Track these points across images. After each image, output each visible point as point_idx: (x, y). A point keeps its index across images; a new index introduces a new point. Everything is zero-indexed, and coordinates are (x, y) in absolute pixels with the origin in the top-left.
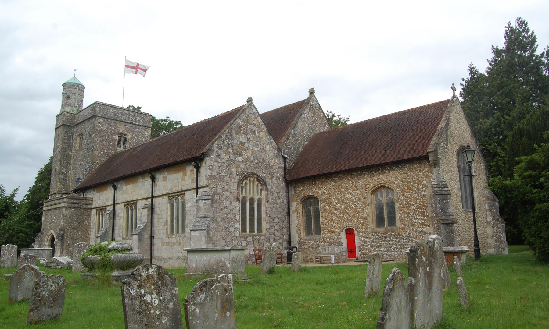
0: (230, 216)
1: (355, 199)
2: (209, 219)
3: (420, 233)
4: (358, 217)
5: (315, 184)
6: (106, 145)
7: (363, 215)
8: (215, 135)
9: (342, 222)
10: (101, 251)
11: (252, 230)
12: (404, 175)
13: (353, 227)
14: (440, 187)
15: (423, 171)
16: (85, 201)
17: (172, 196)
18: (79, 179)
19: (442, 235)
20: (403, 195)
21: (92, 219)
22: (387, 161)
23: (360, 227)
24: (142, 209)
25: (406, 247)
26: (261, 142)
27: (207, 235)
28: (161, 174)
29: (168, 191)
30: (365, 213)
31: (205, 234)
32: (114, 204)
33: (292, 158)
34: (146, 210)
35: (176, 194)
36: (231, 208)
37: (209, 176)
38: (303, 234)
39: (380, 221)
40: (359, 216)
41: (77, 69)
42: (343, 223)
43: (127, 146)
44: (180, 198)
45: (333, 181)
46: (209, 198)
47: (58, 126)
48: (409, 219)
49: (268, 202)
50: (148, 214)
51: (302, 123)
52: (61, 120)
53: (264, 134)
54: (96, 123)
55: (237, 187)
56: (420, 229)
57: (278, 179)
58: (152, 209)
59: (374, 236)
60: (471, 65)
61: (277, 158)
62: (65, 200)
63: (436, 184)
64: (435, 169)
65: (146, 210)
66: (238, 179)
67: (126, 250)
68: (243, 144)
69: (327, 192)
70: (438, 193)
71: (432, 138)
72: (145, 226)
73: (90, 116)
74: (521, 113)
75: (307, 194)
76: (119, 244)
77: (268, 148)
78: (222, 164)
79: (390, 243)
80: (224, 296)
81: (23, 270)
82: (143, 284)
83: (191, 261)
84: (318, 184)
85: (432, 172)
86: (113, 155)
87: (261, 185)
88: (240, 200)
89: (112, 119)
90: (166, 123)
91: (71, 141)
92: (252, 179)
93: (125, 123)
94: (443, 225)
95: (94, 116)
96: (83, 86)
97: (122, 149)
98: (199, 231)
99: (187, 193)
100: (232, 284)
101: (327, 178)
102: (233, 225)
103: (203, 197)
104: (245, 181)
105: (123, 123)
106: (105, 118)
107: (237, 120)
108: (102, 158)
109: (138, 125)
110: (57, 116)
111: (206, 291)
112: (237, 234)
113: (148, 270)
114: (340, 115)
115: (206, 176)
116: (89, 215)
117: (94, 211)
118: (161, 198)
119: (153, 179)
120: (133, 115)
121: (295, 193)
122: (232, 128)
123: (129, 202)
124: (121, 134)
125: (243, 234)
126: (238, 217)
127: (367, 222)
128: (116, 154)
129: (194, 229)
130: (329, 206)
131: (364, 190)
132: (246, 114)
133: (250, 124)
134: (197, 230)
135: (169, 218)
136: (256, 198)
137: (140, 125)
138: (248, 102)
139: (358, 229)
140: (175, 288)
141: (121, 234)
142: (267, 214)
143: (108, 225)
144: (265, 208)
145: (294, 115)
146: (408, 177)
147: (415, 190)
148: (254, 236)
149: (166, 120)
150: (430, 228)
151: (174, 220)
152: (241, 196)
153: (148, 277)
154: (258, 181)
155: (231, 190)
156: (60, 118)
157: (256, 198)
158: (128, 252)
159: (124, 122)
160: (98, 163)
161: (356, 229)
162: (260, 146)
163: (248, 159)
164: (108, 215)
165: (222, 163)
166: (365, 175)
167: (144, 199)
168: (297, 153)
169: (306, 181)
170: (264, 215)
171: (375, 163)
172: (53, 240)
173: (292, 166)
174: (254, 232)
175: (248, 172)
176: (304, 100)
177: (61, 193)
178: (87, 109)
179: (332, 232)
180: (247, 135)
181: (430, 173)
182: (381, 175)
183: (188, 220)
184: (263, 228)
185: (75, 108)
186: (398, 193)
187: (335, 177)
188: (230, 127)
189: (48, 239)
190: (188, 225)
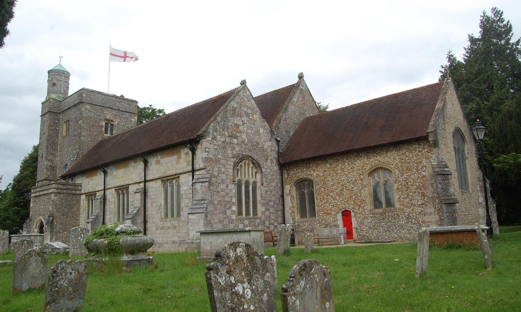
0: (227, 199)
1: (351, 180)
2: (206, 202)
3: (420, 213)
4: (355, 199)
5: (309, 167)
6: (93, 132)
7: (360, 196)
8: (210, 117)
9: (338, 204)
10: (108, 234)
11: (248, 213)
12: (402, 156)
14: (440, 168)
15: (423, 152)
16: (74, 187)
17: (165, 180)
18: (66, 165)
19: (445, 215)
20: (402, 175)
21: (82, 204)
22: (384, 142)
23: (357, 208)
24: (135, 193)
25: (405, 227)
26: (255, 125)
27: (205, 219)
28: (154, 158)
29: (161, 175)
30: (362, 194)
31: (203, 217)
32: (105, 189)
33: (284, 141)
34: (139, 195)
35: (170, 177)
36: (227, 191)
37: (206, 158)
38: (297, 217)
40: (355, 198)
41: (62, 56)
42: (340, 205)
43: (114, 132)
44: (174, 181)
45: (328, 163)
46: (206, 181)
47: (44, 113)
48: (408, 200)
49: (262, 184)
50: (141, 198)
51: (293, 107)
52: (47, 107)
53: (257, 116)
54: (83, 109)
55: (233, 169)
56: (420, 209)
57: (272, 162)
58: (145, 193)
59: (371, 217)
60: (449, 53)
61: (270, 141)
62: (54, 186)
63: (436, 164)
64: (435, 150)
65: (139, 195)
66: (234, 162)
67: (135, 233)
68: (237, 126)
69: (321, 174)
70: (439, 173)
71: (431, 119)
72: (138, 211)
73: (77, 102)
74: (500, 99)
75: (301, 177)
76: (128, 226)
77: (262, 131)
78: (218, 146)
79: (389, 224)
80: (323, 282)
81: (29, 256)
82: (232, 269)
83: (204, 243)
84: (313, 166)
85: (432, 152)
86: (100, 141)
87: (256, 168)
88: (236, 183)
89: (99, 106)
90: (149, 111)
91: (58, 128)
92: (247, 162)
93: (112, 110)
94: (445, 205)
95: (81, 103)
96: (69, 73)
97: (109, 135)
98: (197, 214)
99: (182, 176)
100: (275, 267)
101: (322, 160)
102: (230, 208)
103: (200, 179)
104: (240, 164)
105: (109, 109)
106: (92, 104)
107: (232, 103)
108: (90, 144)
109: (125, 111)
110: (43, 103)
111: (305, 277)
112: (234, 217)
113: (235, 250)
114: (320, 103)
115: (202, 158)
116: (79, 201)
117: (83, 197)
118: (154, 182)
119: (146, 163)
120: (120, 102)
121: (288, 176)
122: (227, 111)
123: (120, 186)
124: (108, 120)
125: (239, 217)
126: (234, 200)
127: (365, 203)
128: (104, 140)
129: (192, 212)
130: (324, 188)
131: (361, 172)
132: (240, 96)
133: (244, 106)
134: (195, 213)
135: (163, 202)
136: (251, 181)
137: (126, 112)
138: (241, 84)
140: (268, 274)
141: (112, 219)
142: (262, 197)
143: (99, 210)
144: (260, 191)
145: (284, 100)
146: (407, 158)
147: (415, 170)
148: (250, 219)
149: (149, 108)
150: (430, 209)
151: (169, 204)
152: (237, 179)
153: (238, 259)
154: (253, 163)
155: (227, 173)
156: (46, 104)
157: (251, 181)
158: (137, 235)
159: (111, 108)
160: (86, 149)
161: (353, 211)
162: (254, 129)
163: (243, 142)
164: (99, 201)
165: (218, 145)
166: (361, 157)
167: (136, 183)
168: (289, 137)
169: (300, 164)
170: (259, 198)
171: (373, 145)
172: (41, 226)
173: (284, 149)
174: (249, 215)
175: (243, 155)
176: (294, 85)
177: (48, 180)
178: (73, 96)
179: (328, 214)
180: (241, 118)
181: (429, 154)
182: (378, 157)
183: (183, 204)
184: (258, 211)
185: (61, 95)
186: (396, 174)
187: (330, 159)
188: (225, 109)
189: (37, 225)
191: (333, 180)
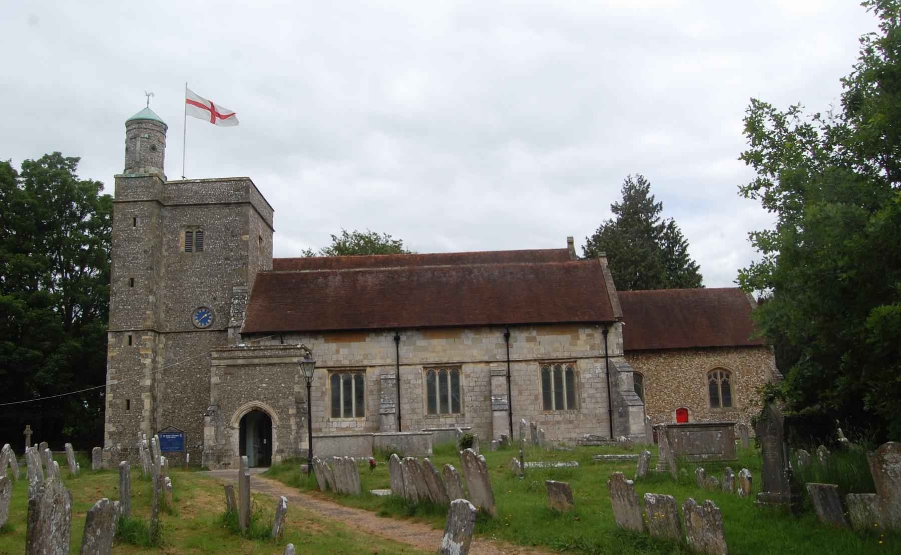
1: (690, 378)
5: (638, 359)
13: (687, 405)
20: (742, 377)
32: (398, 365)
39: (714, 401)
59: (711, 416)
69: (653, 369)
118: (523, 364)
123: (437, 364)
130: (657, 384)
131: (699, 370)
139: (693, 409)
161: (690, 409)
179: (661, 412)
187: (664, 354)
190: (587, 399)
191: (667, 376)
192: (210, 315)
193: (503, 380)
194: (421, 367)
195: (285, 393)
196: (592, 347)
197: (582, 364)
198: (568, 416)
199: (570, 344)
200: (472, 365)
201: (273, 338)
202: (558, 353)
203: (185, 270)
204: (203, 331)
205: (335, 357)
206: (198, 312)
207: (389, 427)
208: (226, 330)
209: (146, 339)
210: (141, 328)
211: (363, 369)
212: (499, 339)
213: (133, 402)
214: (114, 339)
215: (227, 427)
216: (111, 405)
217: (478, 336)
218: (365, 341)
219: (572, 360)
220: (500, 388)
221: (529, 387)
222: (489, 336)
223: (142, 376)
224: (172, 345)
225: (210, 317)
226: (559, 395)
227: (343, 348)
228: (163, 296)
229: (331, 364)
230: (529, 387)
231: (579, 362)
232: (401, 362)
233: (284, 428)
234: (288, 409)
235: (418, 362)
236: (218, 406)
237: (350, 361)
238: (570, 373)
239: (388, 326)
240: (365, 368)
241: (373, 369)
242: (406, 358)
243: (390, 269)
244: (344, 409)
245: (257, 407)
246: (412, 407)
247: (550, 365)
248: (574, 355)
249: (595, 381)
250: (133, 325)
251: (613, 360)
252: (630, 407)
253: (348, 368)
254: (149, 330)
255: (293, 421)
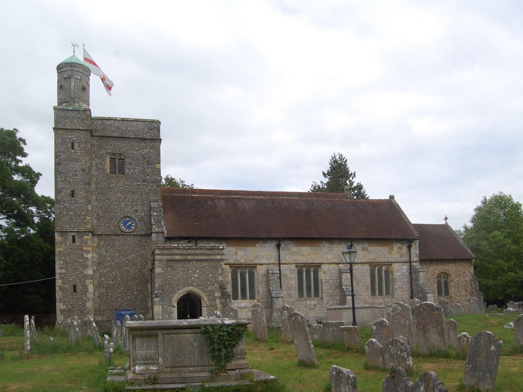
1: (427, 278)
3: (464, 300)
20: (456, 278)
32: (280, 264)
39: (440, 293)
118: (360, 265)
183: (397, 286)
192: (133, 223)
193: (349, 275)
194: (294, 265)
195: (212, 281)
196: (401, 256)
197: (395, 266)
198: (387, 299)
199: (388, 254)
200: (327, 265)
201: (189, 242)
202: (381, 259)
203: (112, 187)
204: (128, 234)
205: (234, 257)
206: (124, 221)
207: (279, 306)
208: (150, 235)
209: (87, 239)
210: (83, 230)
211: (254, 266)
212: (345, 248)
213: (79, 287)
214: (60, 238)
215: (169, 306)
216: (61, 289)
217: (331, 246)
218: (255, 246)
219: (389, 263)
220: (347, 281)
221: (363, 281)
222: (338, 246)
223: (85, 267)
224: (104, 245)
225: (133, 225)
226: (380, 286)
227: (240, 251)
228: (94, 206)
229: (232, 262)
230: (363, 281)
231: (393, 265)
232: (282, 261)
233: (212, 306)
234: (214, 293)
235: (292, 262)
236: (163, 290)
237: (245, 260)
238: (387, 272)
239: (273, 236)
240: (256, 265)
241: (261, 266)
242: (284, 259)
243: (256, 197)
244: (241, 294)
245: (191, 291)
246: (288, 293)
247: (376, 267)
248: (390, 260)
249: (403, 277)
250: (76, 227)
251: (414, 264)
252: (428, 294)
253: (244, 265)
254: (89, 232)
255: (218, 302)
